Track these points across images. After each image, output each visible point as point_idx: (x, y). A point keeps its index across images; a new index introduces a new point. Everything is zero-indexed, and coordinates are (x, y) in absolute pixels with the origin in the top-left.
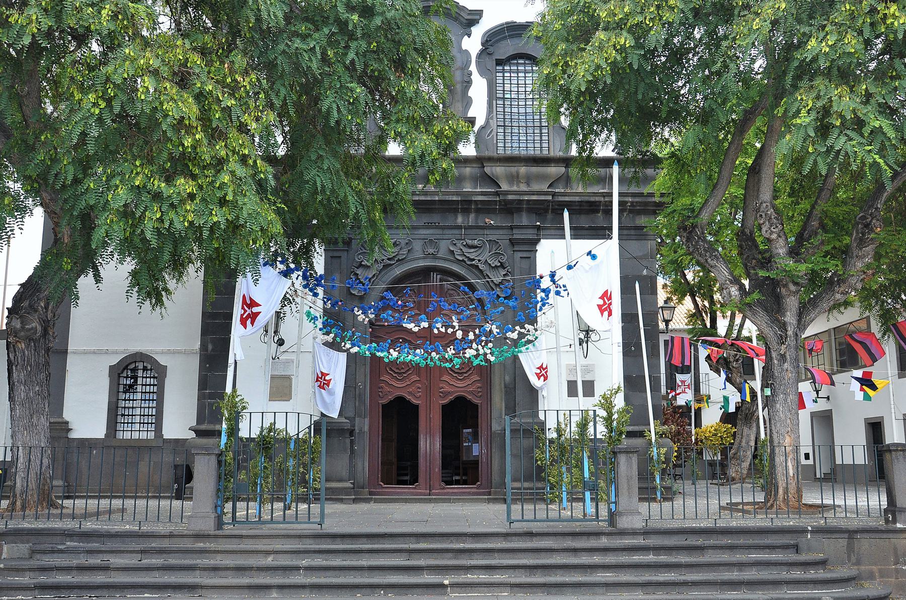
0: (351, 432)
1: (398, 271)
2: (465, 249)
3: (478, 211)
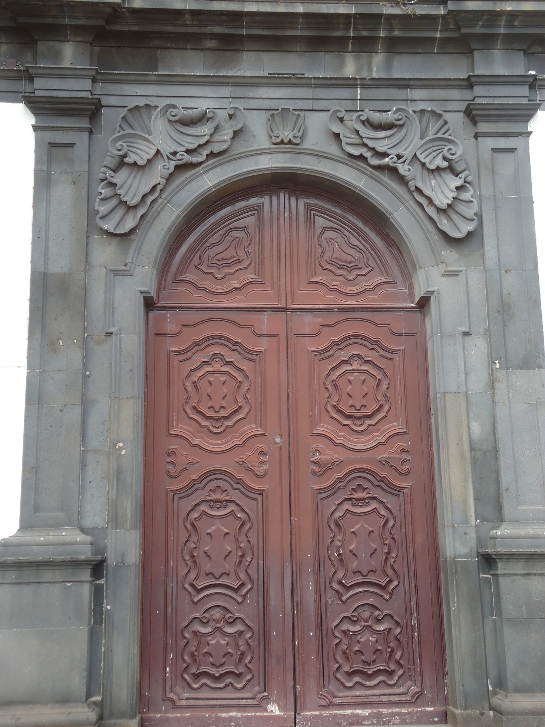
0: (98, 568)
1: (210, 180)
2: (365, 132)
3: (394, 46)
